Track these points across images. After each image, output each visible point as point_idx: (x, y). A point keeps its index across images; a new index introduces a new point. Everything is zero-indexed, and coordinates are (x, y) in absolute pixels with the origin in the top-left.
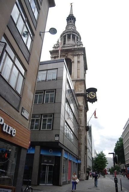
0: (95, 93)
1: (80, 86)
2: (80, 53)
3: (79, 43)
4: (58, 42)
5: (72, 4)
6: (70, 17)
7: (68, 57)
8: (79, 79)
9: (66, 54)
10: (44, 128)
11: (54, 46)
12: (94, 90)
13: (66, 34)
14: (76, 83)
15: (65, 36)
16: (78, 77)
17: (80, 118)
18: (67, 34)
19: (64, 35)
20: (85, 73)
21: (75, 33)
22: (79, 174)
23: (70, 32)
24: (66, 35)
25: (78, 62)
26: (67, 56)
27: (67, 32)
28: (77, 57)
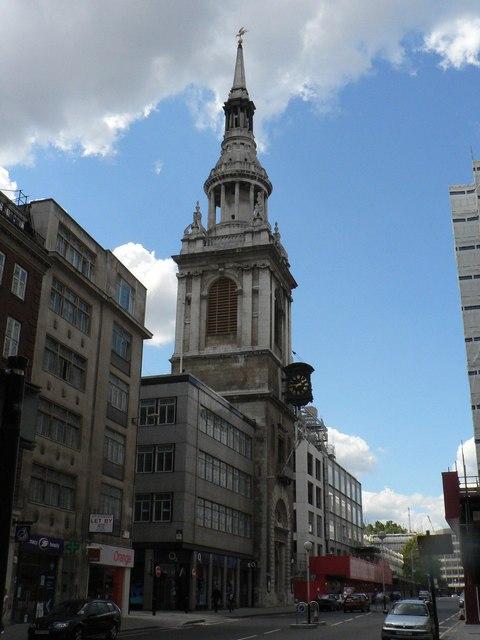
0: (309, 379)
1: (258, 369)
2: (259, 263)
3: (258, 221)
4: (197, 216)
5: (242, 33)
6: (233, 104)
7: (227, 276)
8: (257, 348)
9: (222, 265)
10: (158, 518)
11: (186, 231)
12: (305, 370)
13: (220, 182)
14: (246, 360)
15: (217, 191)
16: (254, 342)
17: (257, 459)
18: (224, 184)
19: (216, 184)
20: (280, 316)
21: (248, 176)
22: (256, 592)
23: (232, 175)
24: (220, 185)
25: (255, 292)
26: (221, 273)
27: (224, 177)
28: (251, 276)
